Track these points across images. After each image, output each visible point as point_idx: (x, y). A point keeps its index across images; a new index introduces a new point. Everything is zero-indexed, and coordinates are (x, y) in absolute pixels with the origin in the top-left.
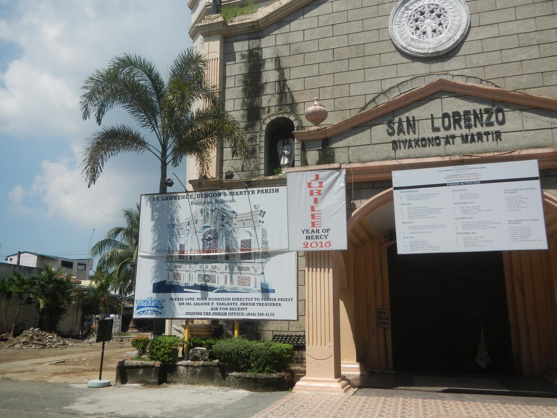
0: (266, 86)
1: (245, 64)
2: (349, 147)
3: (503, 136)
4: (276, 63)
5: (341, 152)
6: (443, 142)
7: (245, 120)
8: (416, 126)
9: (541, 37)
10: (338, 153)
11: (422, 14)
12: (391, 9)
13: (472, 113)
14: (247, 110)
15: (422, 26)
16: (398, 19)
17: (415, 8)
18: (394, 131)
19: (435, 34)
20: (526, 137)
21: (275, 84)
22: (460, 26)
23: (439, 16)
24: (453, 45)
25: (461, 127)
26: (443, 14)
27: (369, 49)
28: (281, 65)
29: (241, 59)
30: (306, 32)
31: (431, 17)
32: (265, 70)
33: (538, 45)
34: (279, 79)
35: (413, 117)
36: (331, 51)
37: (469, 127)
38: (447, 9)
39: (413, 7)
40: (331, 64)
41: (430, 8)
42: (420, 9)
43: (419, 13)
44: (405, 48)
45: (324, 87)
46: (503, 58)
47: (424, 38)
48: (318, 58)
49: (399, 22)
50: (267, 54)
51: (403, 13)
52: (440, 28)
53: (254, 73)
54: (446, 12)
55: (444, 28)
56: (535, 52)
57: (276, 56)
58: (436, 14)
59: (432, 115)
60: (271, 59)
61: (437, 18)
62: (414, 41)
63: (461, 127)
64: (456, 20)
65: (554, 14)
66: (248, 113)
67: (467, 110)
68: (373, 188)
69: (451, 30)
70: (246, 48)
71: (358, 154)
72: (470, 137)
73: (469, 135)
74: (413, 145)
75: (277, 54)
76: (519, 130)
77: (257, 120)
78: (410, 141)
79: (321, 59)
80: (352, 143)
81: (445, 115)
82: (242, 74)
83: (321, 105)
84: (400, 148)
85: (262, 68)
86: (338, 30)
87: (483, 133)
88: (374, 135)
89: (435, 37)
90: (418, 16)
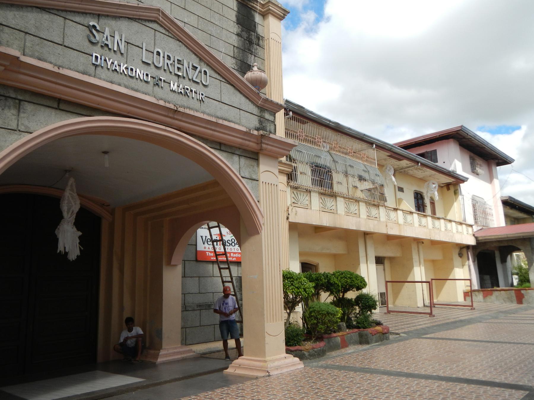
65: (185, 9)
68: (56, 109)
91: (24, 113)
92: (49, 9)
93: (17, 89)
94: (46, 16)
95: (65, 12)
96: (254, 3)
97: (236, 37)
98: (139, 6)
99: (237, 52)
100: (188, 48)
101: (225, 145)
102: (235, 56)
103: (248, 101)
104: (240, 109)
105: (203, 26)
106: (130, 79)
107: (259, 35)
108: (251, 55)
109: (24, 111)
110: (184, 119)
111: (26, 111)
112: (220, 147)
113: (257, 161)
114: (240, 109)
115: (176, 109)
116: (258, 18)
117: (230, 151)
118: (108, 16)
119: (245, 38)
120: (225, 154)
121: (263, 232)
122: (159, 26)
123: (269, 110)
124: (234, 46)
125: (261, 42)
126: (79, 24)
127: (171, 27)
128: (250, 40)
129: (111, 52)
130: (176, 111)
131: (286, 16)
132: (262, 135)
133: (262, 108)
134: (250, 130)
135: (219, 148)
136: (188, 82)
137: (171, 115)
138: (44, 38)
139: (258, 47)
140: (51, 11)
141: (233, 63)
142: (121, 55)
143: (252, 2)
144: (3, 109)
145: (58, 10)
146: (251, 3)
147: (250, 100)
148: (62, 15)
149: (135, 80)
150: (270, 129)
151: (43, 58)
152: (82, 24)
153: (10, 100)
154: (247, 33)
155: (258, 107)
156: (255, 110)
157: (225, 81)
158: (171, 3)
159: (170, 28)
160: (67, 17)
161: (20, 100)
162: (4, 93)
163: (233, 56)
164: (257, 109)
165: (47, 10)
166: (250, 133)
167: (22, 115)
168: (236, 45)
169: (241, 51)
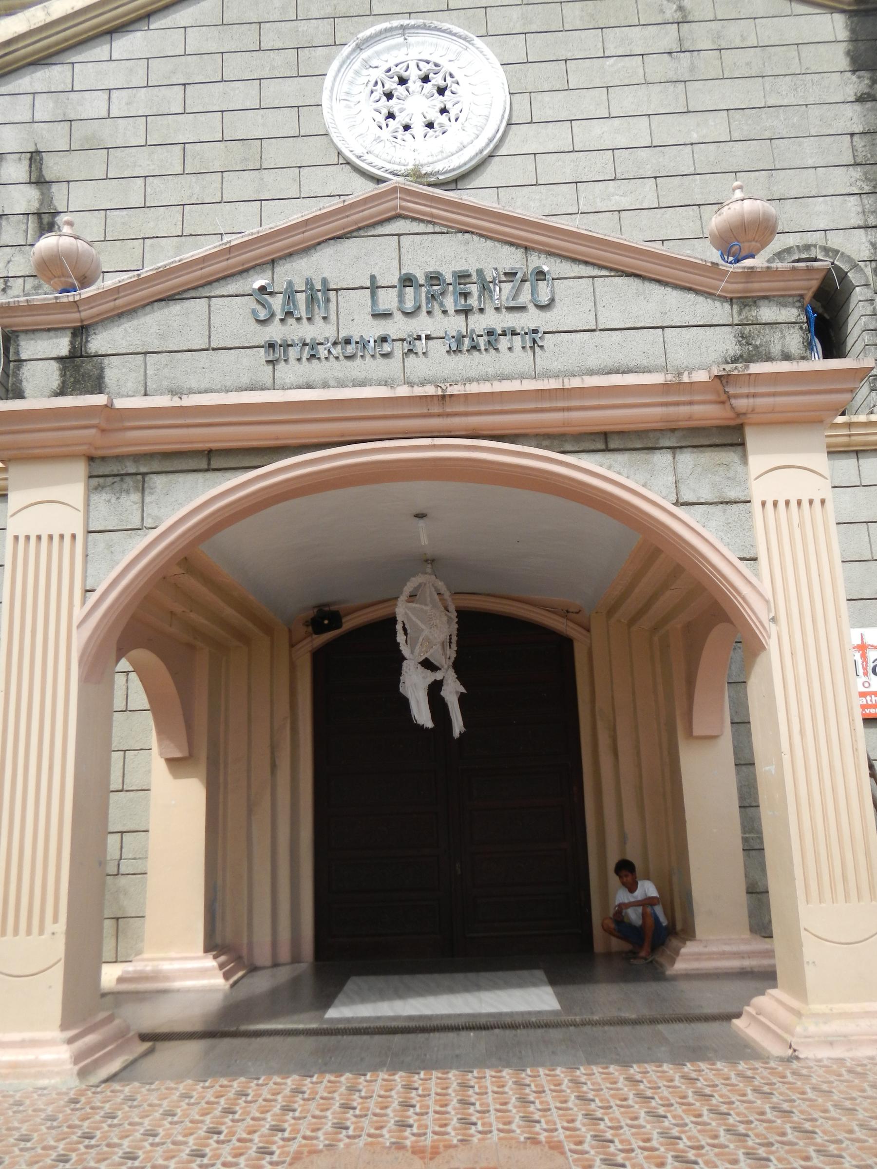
4: (30, 166)
5: (124, 367)
6: (399, 349)
8: (332, 306)
9: (661, 160)
10: (115, 370)
11: (403, 81)
12: (329, 60)
13: (474, 278)
15: (401, 111)
16: (345, 87)
17: (386, 68)
18: (273, 315)
19: (431, 132)
21: (25, 221)
22: (487, 118)
23: (441, 91)
24: (471, 159)
25: (445, 312)
26: (451, 87)
27: (274, 153)
28: (44, 172)
30: (115, 94)
33: (655, 178)
34: (38, 209)
35: (325, 281)
37: (466, 312)
40: (176, 181)
41: (420, 70)
42: (398, 69)
43: (396, 79)
44: (359, 157)
45: (157, 237)
46: (581, 202)
47: (405, 138)
48: (145, 163)
52: (444, 118)
54: (458, 83)
55: (453, 119)
56: (647, 194)
58: (434, 85)
59: (373, 278)
60: (18, 155)
61: (436, 95)
62: (382, 143)
63: (445, 312)
67: (463, 268)
68: (207, 470)
69: (466, 124)
72: (467, 341)
73: (464, 337)
76: (587, 328)
78: (314, 345)
79: (152, 167)
81: (407, 281)
83: (77, 238)
86: (198, 98)
88: (216, 325)
89: (431, 137)
90: (392, 84)
91: (151, 493)
92: (179, 293)
93: (137, 458)
94: (176, 308)
95: (209, 286)
97: (857, 107)
98: (346, 203)
99: (865, 146)
100: (487, 238)
101: (621, 433)
102: (859, 160)
103: (691, 296)
105: (745, 128)
106: (349, 363)
109: (152, 491)
110: (471, 409)
112: (606, 443)
113: (740, 448)
114: (663, 328)
115: (440, 393)
117: (638, 446)
118: (290, 255)
121: (772, 645)
122: (408, 222)
123: (774, 296)
124: (852, 135)
126: (237, 296)
127: (434, 211)
129: (302, 324)
130: (443, 397)
132: (719, 377)
134: (680, 374)
135: (603, 447)
136: (493, 318)
137: (436, 410)
138: (176, 349)
140: (184, 296)
141: (853, 180)
142: (325, 322)
144: (118, 498)
145: (195, 288)
147: (697, 292)
148: (204, 295)
149: (359, 361)
150: (783, 345)
151: (178, 387)
152: (242, 293)
153: (128, 479)
155: (723, 299)
156: (721, 312)
159: (432, 215)
160: (213, 294)
161: (144, 475)
162: (118, 470)
164: (727, 306)
165: (177, 297)
167: (148, 499)
168: (858, 129)
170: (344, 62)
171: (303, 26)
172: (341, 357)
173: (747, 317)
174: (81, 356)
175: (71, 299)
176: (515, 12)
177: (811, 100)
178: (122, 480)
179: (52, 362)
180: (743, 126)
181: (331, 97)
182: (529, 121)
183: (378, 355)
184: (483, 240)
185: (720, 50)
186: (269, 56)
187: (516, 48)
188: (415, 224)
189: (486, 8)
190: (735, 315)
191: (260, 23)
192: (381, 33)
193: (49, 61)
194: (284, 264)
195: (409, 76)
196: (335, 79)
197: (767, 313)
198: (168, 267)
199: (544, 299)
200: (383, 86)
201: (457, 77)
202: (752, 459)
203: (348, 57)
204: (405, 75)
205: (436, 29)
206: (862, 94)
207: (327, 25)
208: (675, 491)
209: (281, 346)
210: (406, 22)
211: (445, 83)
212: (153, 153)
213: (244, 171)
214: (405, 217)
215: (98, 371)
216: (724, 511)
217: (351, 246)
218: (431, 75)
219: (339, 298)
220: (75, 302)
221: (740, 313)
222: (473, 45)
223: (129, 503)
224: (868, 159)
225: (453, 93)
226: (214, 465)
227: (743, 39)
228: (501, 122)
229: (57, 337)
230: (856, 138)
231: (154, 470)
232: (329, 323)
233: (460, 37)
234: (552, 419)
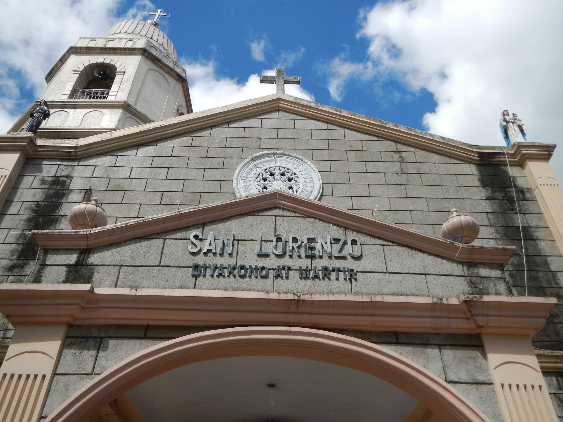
0: (61, 220)
1: (44, 190)
2: (121, 266)
3: (360, 276)
4: (85, 195)
5: (106, 272)
6: (271, 274)
7: (15, 257)
9: (395, 216)
10: (100, 274)
12: (238, 164)
14: (23, 244)
15: (270, 186)
16: (244, 175)
17: (265, 168)
20: (391, 282)
22: (311, 192)
23: (290, 180)
26: (295, 178)
29: (40, 185)
31: (281, 180)
32: (67, 201)
36: (159, 194)
38: (298, 174)
39: (262, 166)
41: (281, 171)
43: (269, 173)
48: (142, 198)
49: (245, 177)
50: (76, 184)
51: (251, 169)
53: (52, 202)
54: (298, 177)
57: (88, 188)
60: (80, 191)
61: (287, 181)
63: (300, 256)
64: (308, 186)
66: (22, 249)
70: (52, 174)
71: (134, 279)
72: (312, 272)
73: (310, 270)
74: (226, 275)
75: (90, 187)
76: (381, 271)
77: (32, 260)
78: (222, 268)
79: (145, 200)
80: (129, 260)
82: (34, 202)
84: (204, 276)
85: (65, 198)
87: (331, 269)
88: (166, 253)
93: (100, 327)
94: (145, 244)
96: (499, 158)
97: (487, 202)
98: (248, 198)
99: (494, 218)
100: (324, 221)
101: (406, 333)
102: (492, 224)
103: (439, 259)
104: (425, 274)
105: (435, 206)
106: (241, 280)
107: (522, 188)
108: (516, 215)
109: (105, 349)
111: (106, 349)
112: (397, 339)
114: (425, 274)
115: (296, 298)
116: (512, 171)
117: (417, 342)
119: (502, 198)
120: (408, 349)
122: (281, 210)
124: (487, 213)
125: (528, 195)
126: (181, 239)
128: (509, 198)
129: (216, 256)
131: (553, 151)
133: (471, 262)
135: (396, 341)
136: (327, 261)
138: (139, 265)
139: (524, 202)
140: (151, 237)
141: (491, 232)
143: (496, 158)
144: (81, 352)
146: (495, 159)
147: (443, 258)
148: (162, 238)
149: (247, 278)
154: (501, 192)
155: (458, 262)
156: (457, 269)
157: (391, 244)
158: (389, 197)
159: (295, 208)
160: (167, 237)
161: (102, 338)
163: (488, 224)
164: (460, 266)
165: (146, 237)
166: (442, 304)
168: (490, 211)
169: (500, 214)
170: (245, 165)
171: (228, 150)
172: (237, 276)
173: (472, 273)
174: (82, 265)
175: (85, 233)
176: (325, 153)
177: (465, 197)
178: (87, 341)
179: (64, 267)
180: (433, 205)
181: (238, 178)
182: (332, 195)
183: (259, 277)
184: (322, 222)
185: (420, 174)
186: (211, 160)
187: (326, 166)
188: (285, 212)
189: (312, 150)
190: (466, 272)
191: (208, 147)
192: (264, 155)
193: (107, 154)
194: (210, 226)
195: (275, 173)
196: (240, 171)
197: (484, 272)
198: (145, 221)
199: (357, 254)
200: (263, 176)
201: (298, 175)
202: (490, 356)
203: (247, 163)
204: (273, 172)
205: (289, 155)
206: (489, 196)
207: (239, 151)
208: (443, 373)
209: (202, 267)
210: (275, 152)
211: (292, 177)
212: (147, 194)
213: (190, 205)
214: (280, 208)
215: (90, 274)
216: (478, 389)
217: (249, 220)
218: (285, 173)
219: (239, 244)
220: (87, 234)
221: (468, 270)
222: (306, 163)
223: (87, 356)
224: (497, 224)
225: (295, 181)
226: (149, 335)
227: (430, 171)
228: (318, 194)
229: (70, 254)
230: (489, 215)
231: (110, 335)
232: (232, 257)
233: (300, 159)
234: (364, 322)
